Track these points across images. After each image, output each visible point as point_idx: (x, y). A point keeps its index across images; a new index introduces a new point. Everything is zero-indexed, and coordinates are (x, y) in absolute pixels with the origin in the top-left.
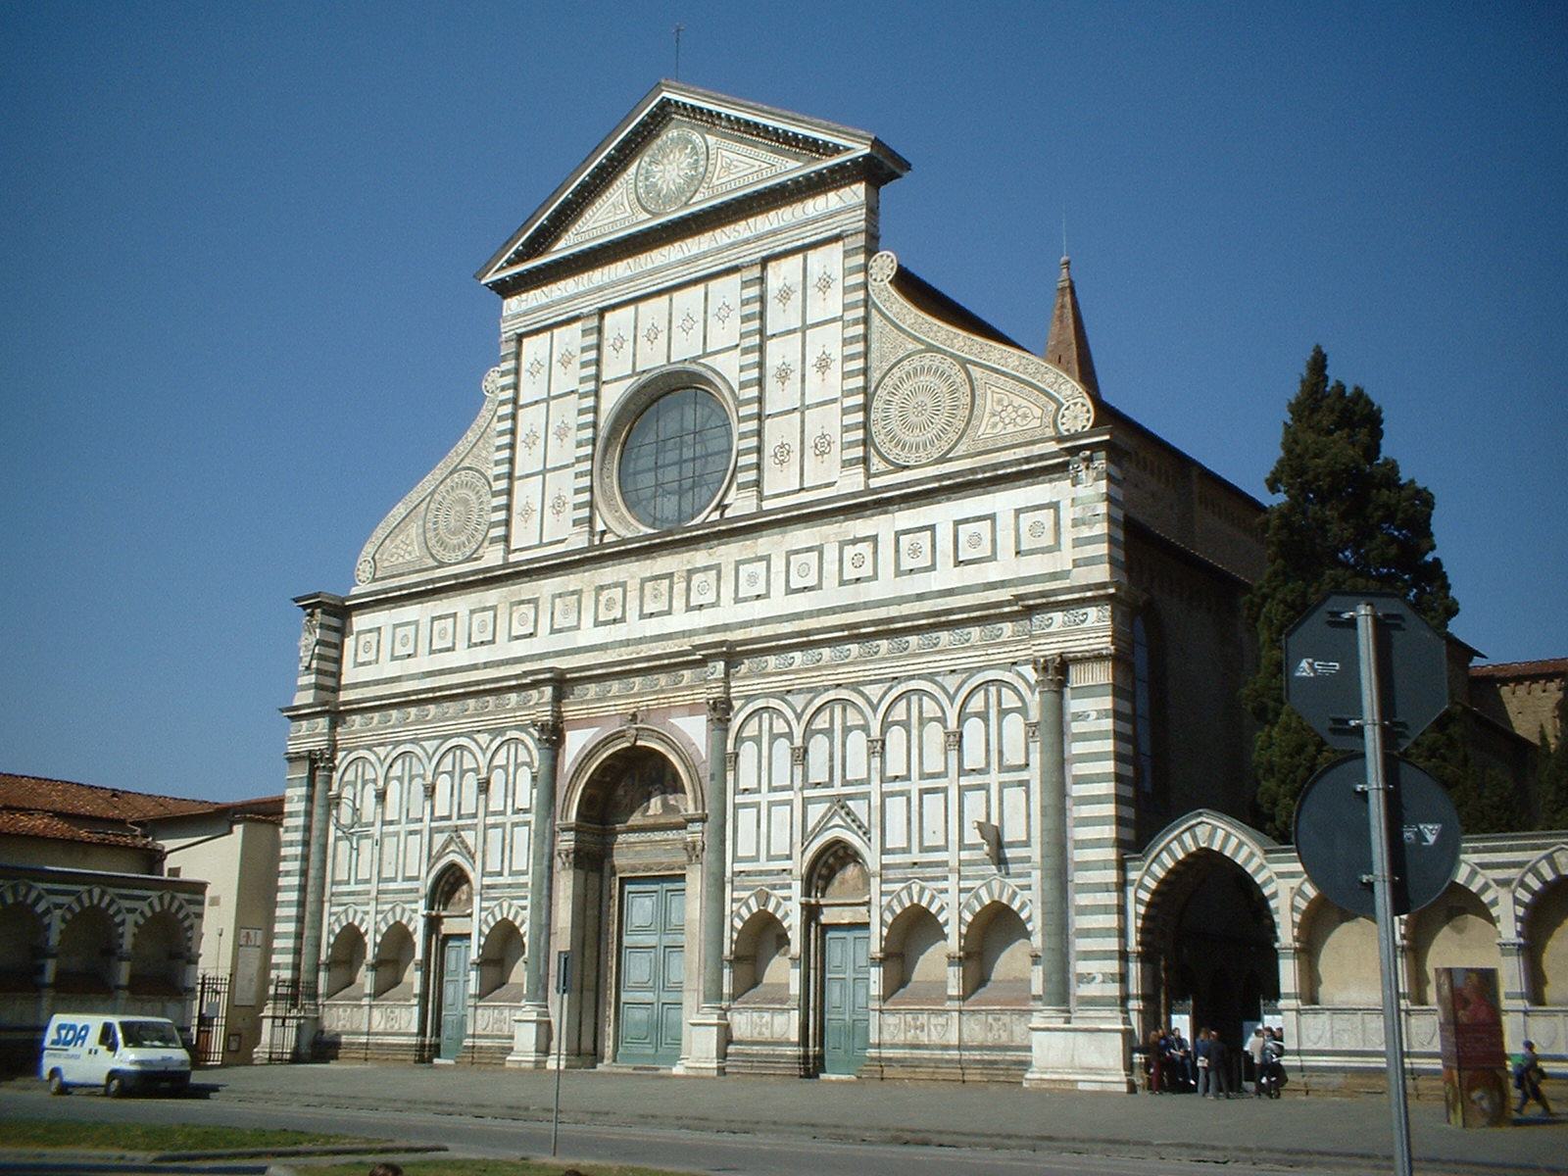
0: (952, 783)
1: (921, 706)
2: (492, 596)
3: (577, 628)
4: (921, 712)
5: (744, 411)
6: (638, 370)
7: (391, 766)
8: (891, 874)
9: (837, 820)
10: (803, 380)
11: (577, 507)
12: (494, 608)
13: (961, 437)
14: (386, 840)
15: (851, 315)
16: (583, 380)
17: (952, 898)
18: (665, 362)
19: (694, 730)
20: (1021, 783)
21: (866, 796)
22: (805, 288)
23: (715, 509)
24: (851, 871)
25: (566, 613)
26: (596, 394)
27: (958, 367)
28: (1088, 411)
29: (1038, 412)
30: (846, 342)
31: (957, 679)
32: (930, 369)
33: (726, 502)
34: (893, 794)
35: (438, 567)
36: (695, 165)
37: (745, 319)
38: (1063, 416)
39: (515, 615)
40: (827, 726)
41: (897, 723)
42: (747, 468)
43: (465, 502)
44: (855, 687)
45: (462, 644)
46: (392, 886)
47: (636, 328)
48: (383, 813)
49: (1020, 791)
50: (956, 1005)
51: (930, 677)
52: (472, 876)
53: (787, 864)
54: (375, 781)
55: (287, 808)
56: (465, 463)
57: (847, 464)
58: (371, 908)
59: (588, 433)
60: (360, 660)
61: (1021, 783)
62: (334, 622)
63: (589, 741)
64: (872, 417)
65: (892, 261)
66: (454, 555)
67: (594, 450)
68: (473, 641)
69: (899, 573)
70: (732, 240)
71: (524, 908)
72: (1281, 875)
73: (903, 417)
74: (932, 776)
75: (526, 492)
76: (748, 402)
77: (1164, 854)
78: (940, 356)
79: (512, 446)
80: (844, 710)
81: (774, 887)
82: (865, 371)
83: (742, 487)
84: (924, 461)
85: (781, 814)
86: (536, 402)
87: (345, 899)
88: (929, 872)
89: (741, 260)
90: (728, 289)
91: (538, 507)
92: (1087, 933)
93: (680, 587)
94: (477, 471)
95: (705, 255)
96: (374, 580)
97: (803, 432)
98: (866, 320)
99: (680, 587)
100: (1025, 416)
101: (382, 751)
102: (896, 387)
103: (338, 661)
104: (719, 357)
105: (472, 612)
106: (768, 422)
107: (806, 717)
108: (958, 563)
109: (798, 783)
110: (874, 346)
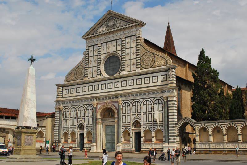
0: (153, 113)
3: (98, 90)
5: (122, 59)
7: (71, 109)
8: (144, 125)
9: (136, 118)
10: (131, 55)
11: (98, 72)
15: (137, 46)
16: (99, 54)
17: (153, 128)
21: (141, 114)
24: (139, 125)
26: (101, 56)
29: (164, 62)
30: (137, 50)
36: (114, 23)
41: (145, 105)
44: (139, 99)
45: (81, 91)
46: (72, 127)
50: (154, 143)
51: (149, 98)
52: (84, 125)
53: (129, 124)
54: (69, 112)
55: (55, 115)
56: (81, 65)
57: (137, 68)
58: (69, 130)
59: (100, 61)
61: (162, 113)
62: (61, 88)
63: (101, 106)
69: (145, 84)
71: (92, 130)
72: (196, 126)
74: (149, 112)
75: (90, 70)
77: (181, 123)
79: (88, 63)
81: (128, 127)
82: (140, 55)
85: (129, 117)
87: (64, 128)
88: (149, 125)
90: (119, 42)
92: (171, 133)
96: (67, 82)
98: (140, 47)
101: (70, 107)
103: (62, 94)
104: (119, 51)
106: (126, 61)
107: (132, 104)
109: (131, 112)
110: (141, 51)
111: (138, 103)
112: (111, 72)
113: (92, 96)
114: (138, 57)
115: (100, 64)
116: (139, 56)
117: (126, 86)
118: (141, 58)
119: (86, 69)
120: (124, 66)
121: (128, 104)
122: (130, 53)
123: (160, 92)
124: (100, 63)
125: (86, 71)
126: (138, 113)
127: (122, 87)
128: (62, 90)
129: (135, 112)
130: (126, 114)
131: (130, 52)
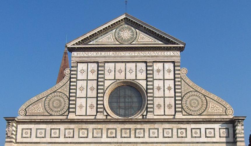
2: (72, 126)
3: (101, 137)
5: (148, 95)
12: (73, 129)
25: (97, 133)
26: (104, 82)
27: (203, 96)
28: (233, 111)
29: (222, 109)
32: (196, 95)
35: (50, 116)
37: (147, 74)
38: (227, 111)
42: (151, 108)
43: (60, 101)
47: (115, 68)
56: (59, 90)
59: (102, 91)
60: (23, 136)
62: (15, 125)
64: (183, 103)
65: (186, 70)
66: (56, 113)
67: (104, 95)
70: (144, 55)
73: (191, 105)
76: (150, 93)
79: (76, 89)
83: (147, 112)
84: (196, 114)
89: (148, 60)
91: (85, 106)
93: (133, 132)
94: (63, 93)
95: (137, 56)
96: (26, 115)
97: (164, 102)
99: (133, 132)
100: (219, 109)
102: (188, 97)
105: (65, 129)
106: (155, 98)
108: (206, 137)
112: (122, 112)
114: (178, 96)
115: (102, 95)
116: (180, 94)
117: (158, 137)
118: (182, 98)
119: (71, 98)
120: (152, 106)
124: (104, 93)
127: (149, 137)
128: (15, 129)
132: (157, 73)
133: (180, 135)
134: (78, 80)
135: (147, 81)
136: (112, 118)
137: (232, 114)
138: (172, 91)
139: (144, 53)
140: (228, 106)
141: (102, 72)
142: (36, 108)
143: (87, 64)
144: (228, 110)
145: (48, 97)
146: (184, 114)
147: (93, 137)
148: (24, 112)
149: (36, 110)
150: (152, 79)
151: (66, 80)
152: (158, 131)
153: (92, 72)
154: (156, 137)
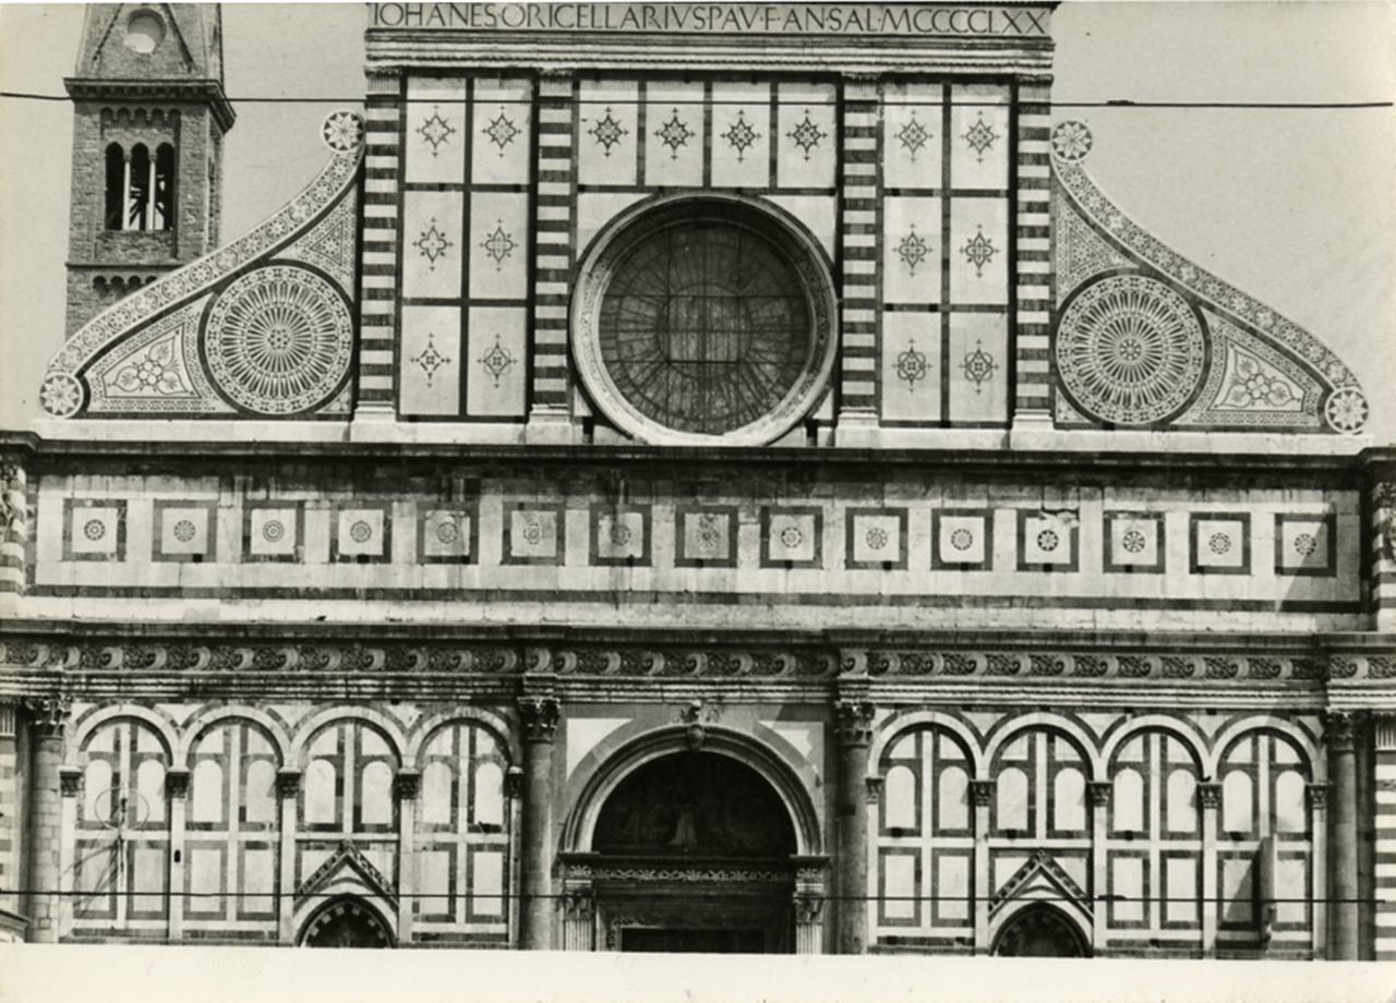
1: (1164, 747)
4: (1164, 754)
5: (850, 292)
6: (650, 181)
7: (199, 737)
9: (1041, 881)
13: (1190, 402)
14: (196, 855)
18: (700, 184)
19: (802, 742)
20: (1299, 855)
21: (1089, 854)
22: (947, 135)
23: (796, 425)
25: (532, 537)
27: (1186, 306)
29: (1298, 393)
31: (1219, 720)
33: (816, 416)
34: (1123, 854)
37: (842, 157)
39: (428, 523)
40: (1024, 757)
43: (298, 321)
48: (189, 811)
49: (1298, 867)
51: (1179, 713)
52: (391, 917)
56: (290, 253)
59: (560, 262)
61: (1299, 855)
64: (1059, 344)
66: (273, 402)
68: (343, 549)
70: (826, 30)
74: (1174, 836)
78: (1159, 285)
80: (1051, 740)
82: (1048, 280)
83: (840, 402)
84: (1136, 422)
86: (442, 187)
96: (83, 413)
97: (945, 341)
100: (1281, 395)
106: (887, 316)
111: (1057, 739)
113: (512, 629)
114: (1031, 305)
115: (561, 288)
116: (1042, 293)
118: (1057, 317)
119: (370, 307)
121: (945, 741)
122: (936, 244)
123: (1287, 669)
125: (368, 333)
126: (1052, 833)
127: (851, 563)
129: (1022, 825)
130: (927, 842)
131: (938, 231)
132: (907, 150)
133: (1034, 554)
134: (411, 187)
135: (843, 205)
136: (623, 441)
137: (1358, 425)
138: (998, 268)
139: (827, 15)
140: (1335, 373)
141: (563, 140)
142: (148, 366)
143: (464, 82)
144: (1337, 401)
145: (224, 295)
146: (1062, 416)
147: (508, 559)
148: (76, 390)
149: (152, 380)
150: (870, 192)
151: (336, 184)
152: (904, 527)
153: (501, 135)
154: (887, 566)
